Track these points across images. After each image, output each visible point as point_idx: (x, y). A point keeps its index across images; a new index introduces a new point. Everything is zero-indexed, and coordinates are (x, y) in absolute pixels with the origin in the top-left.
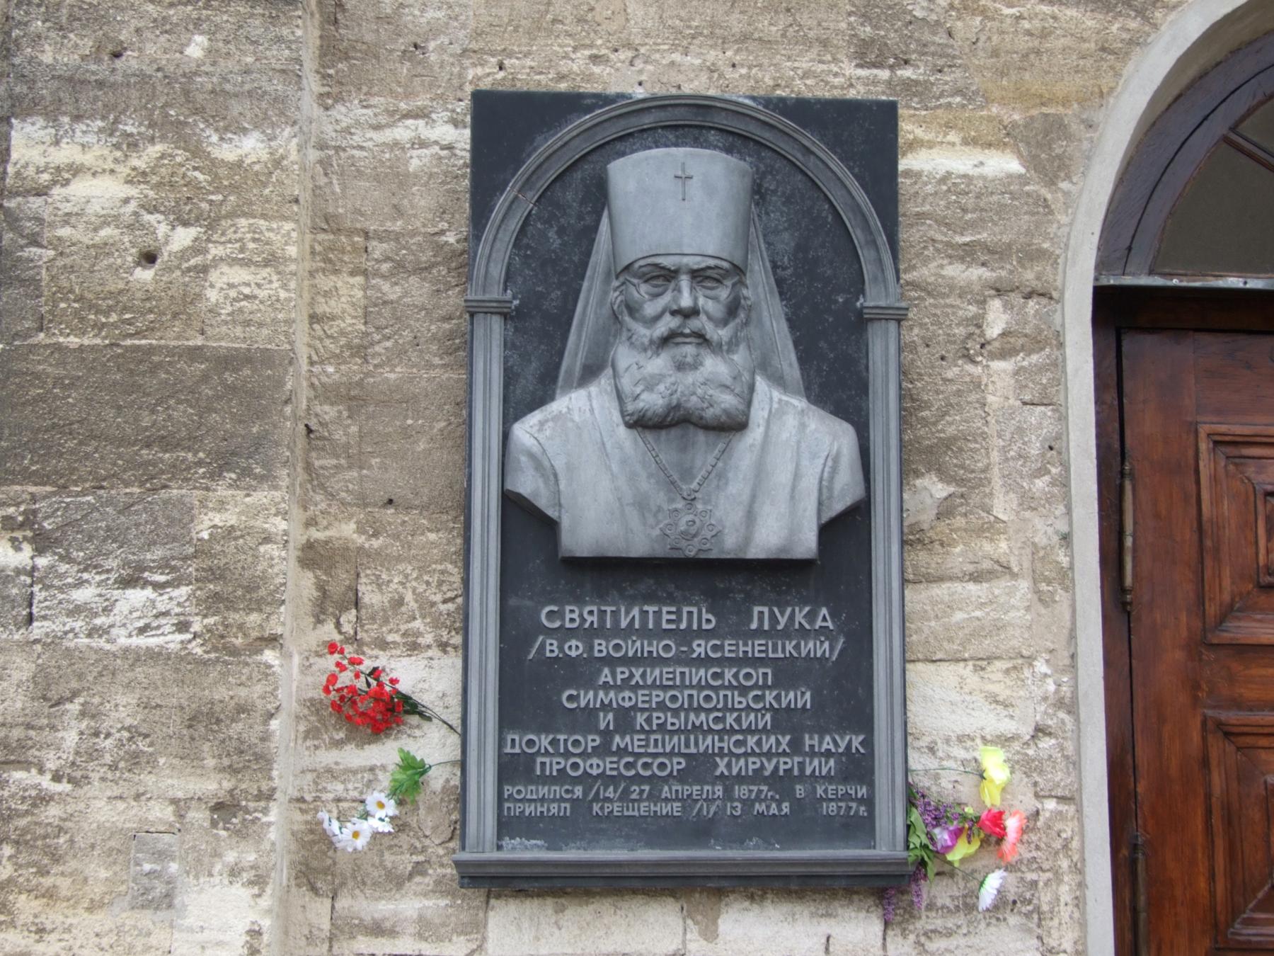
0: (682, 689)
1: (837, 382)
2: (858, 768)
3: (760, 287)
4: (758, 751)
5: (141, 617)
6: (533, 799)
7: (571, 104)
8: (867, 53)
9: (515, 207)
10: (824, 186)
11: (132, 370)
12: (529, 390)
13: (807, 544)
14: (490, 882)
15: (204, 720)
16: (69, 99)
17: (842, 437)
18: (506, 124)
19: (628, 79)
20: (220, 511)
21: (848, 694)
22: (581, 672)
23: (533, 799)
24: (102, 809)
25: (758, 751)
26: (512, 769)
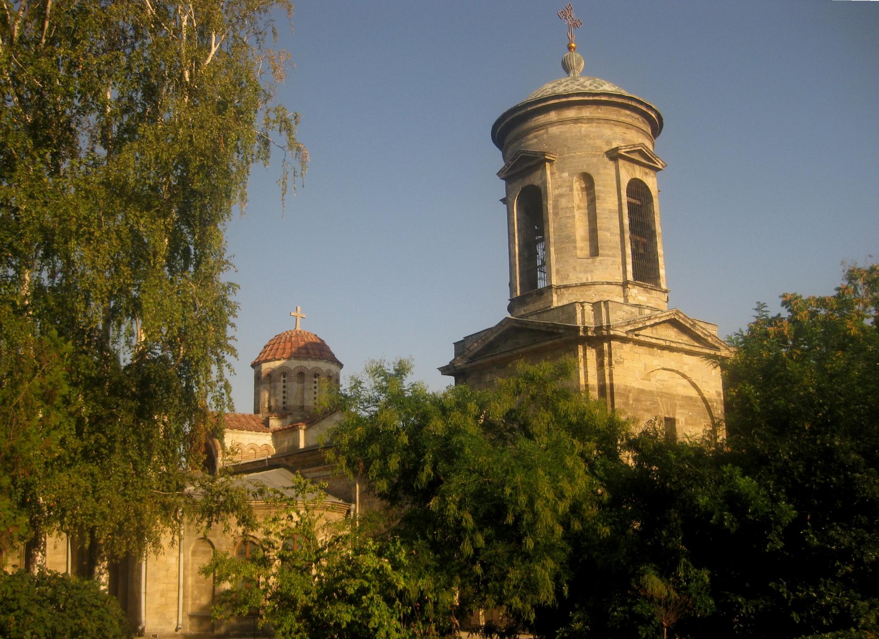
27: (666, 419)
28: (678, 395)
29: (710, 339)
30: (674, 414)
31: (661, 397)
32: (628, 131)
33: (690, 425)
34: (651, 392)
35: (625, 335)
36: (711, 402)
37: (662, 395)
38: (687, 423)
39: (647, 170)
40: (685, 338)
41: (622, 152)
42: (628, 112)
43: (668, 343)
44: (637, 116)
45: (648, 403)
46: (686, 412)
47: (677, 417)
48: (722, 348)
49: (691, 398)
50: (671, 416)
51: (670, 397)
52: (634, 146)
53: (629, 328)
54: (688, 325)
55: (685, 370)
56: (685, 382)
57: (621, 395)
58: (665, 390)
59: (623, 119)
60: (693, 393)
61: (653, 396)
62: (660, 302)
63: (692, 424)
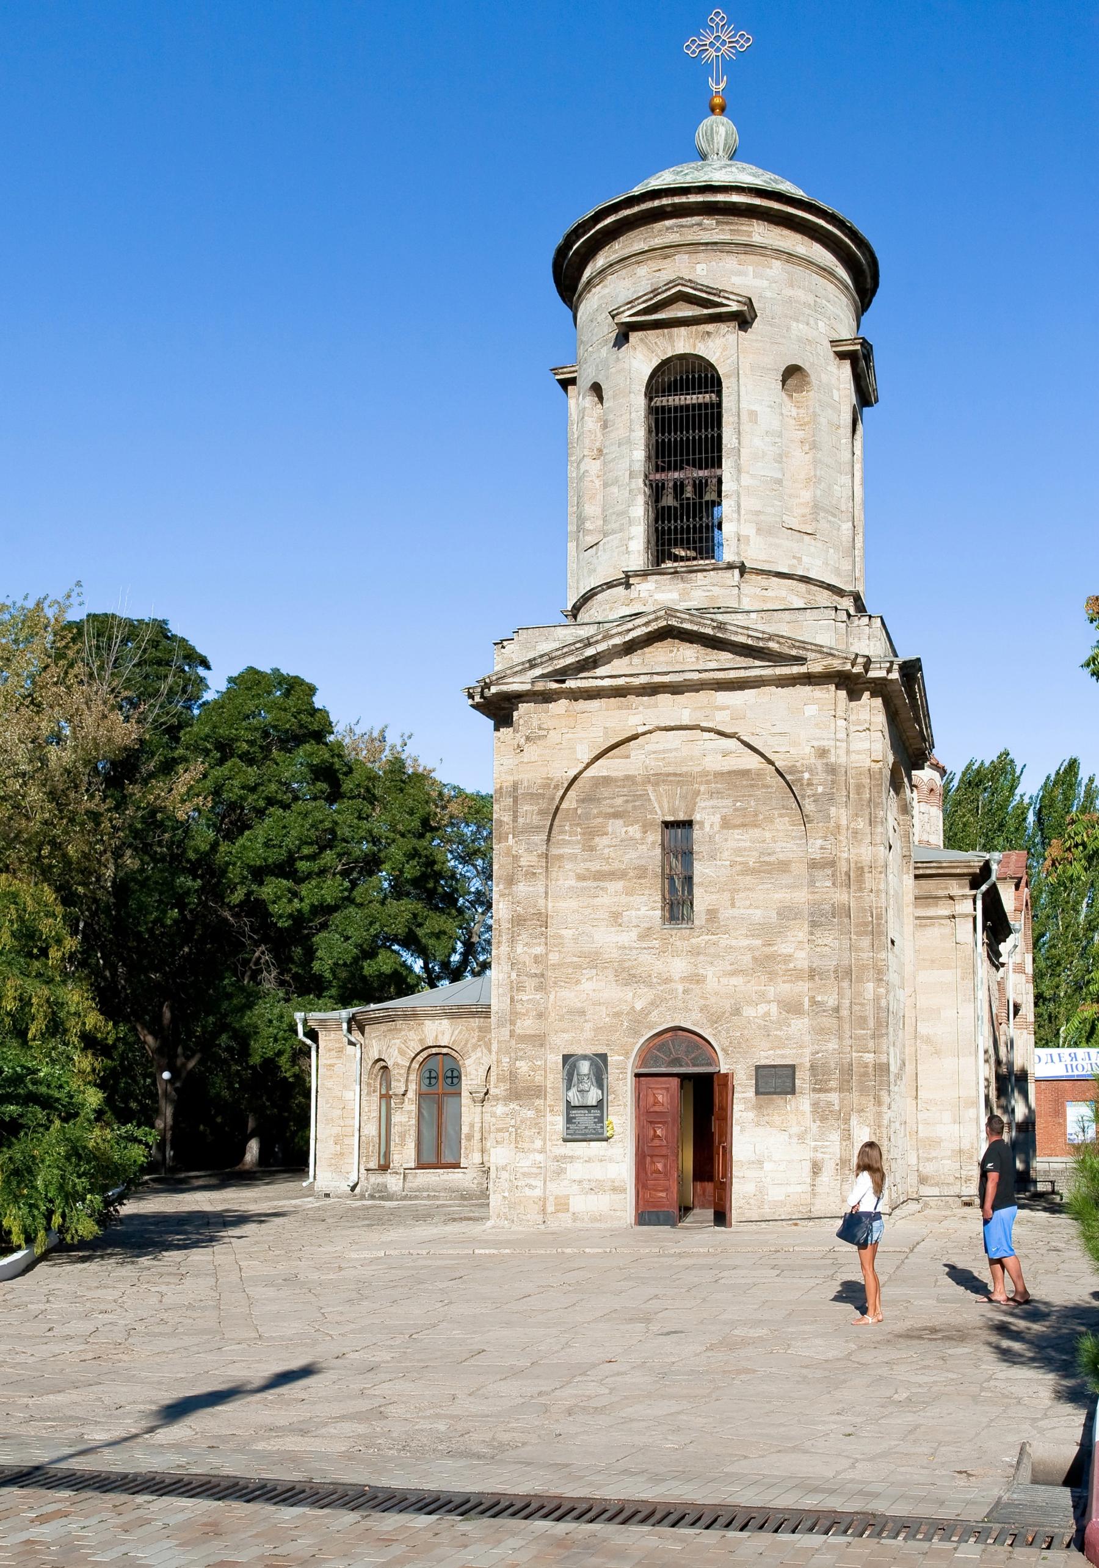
0: (585, 1120)
1: (600, 1085)
2: (602, 1127)
3: (592, 1076)
4: (592, 1126)
5: (531, 1114)
6: (569, 1131)
7: (572, 1055)
8: (608, 1045)
9: (567, 1067)
10: (600, 1063)
11: (528, 1089)
12: (569, 1089)
13: (594, 1104)
14: (565, 1140)
15: (536, 1124)
16: (522, 1058)
17: (600, 1092)
18: (566, 1058)
19: (580, 1052)
20: (538, 1102)
21: (601, 1120)
22: (574, 1118)
23: (569, 1131)
24: (527, 1133)
25: (592, 1126)
26: (568, 1128)
27: (667, 825)
28: (705, 774)
29: (772, 645)
30: (693, 810)
31: (656, 784)
32: (666, 264)
33: (736, 827)
34: (627, 778)
35: (528, 687)
36: (793, 770)
37: (658, 779)
38: (726, 824)
39: (710, 327)
40: (725, 658)
41: (625, 318)
42: (668, 223)
43: (643, 680)
44: (696, 219)
45: (619, 801)
46: (728, 802)
47: (697, 817)
48: (810, 655)
49: (745, 773)
50: (682, 817)
51: (679, 779)
52: (655, 292)
53: (538, 672)
54: (709, 631)
55: (721, 720)
56: (732, 743)
57: (533, 797)
58: (670, 770)
59: (657, 242)
60: (753, 762)
61: (634, 783)
62: (716, 591)
63: (744, 825)
